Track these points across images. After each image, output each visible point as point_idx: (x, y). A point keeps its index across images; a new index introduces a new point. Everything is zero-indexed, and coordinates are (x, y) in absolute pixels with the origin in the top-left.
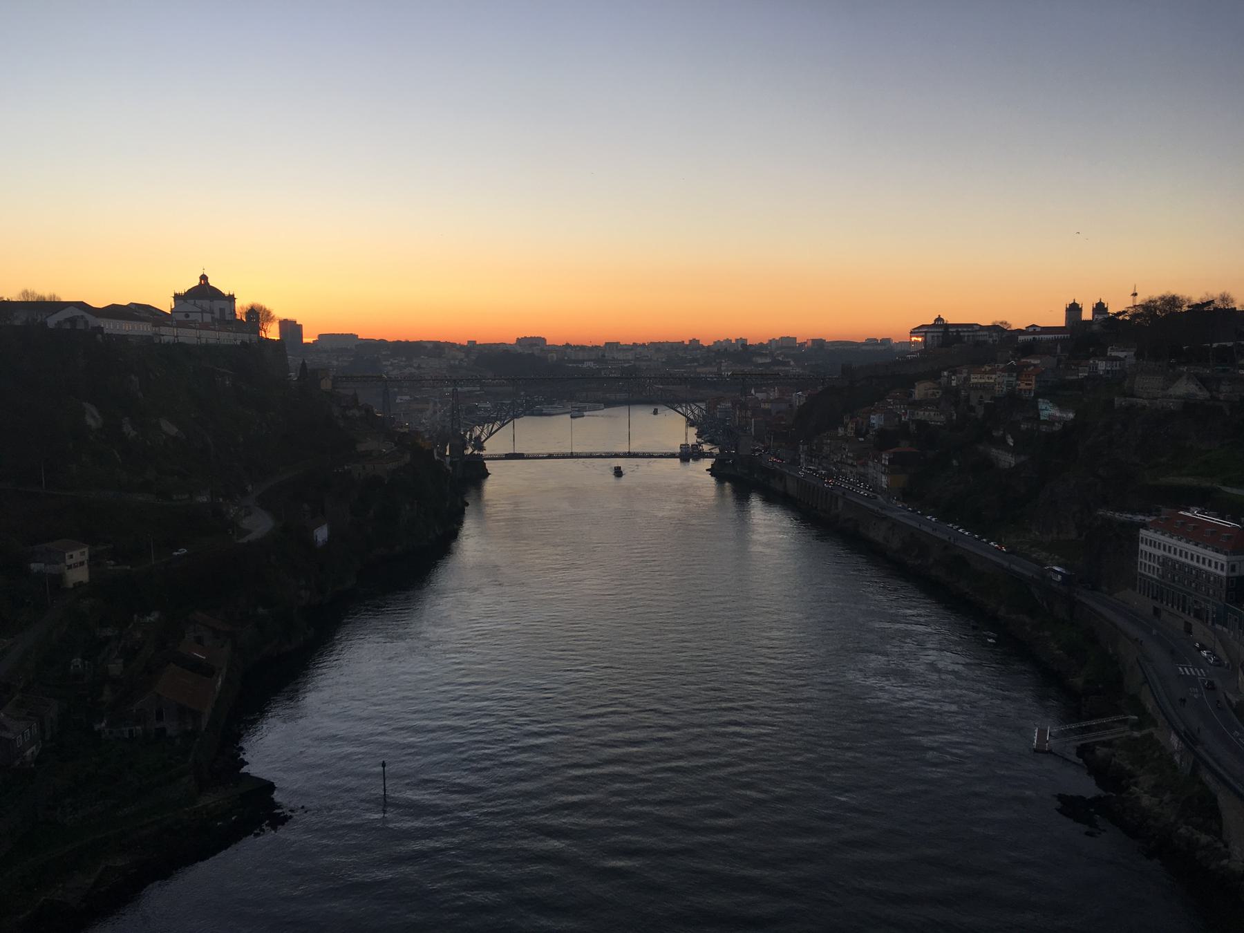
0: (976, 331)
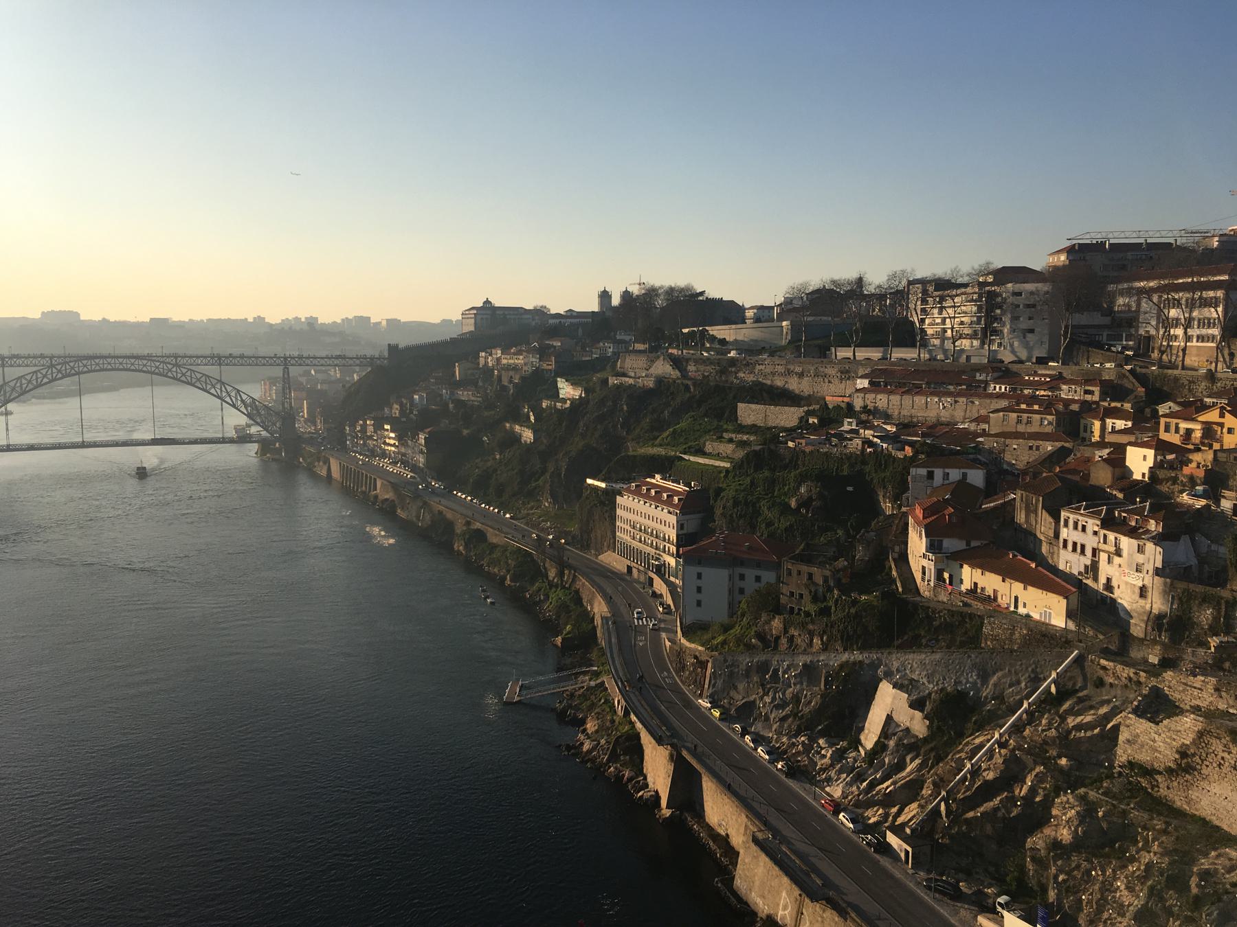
0: (522, 314)
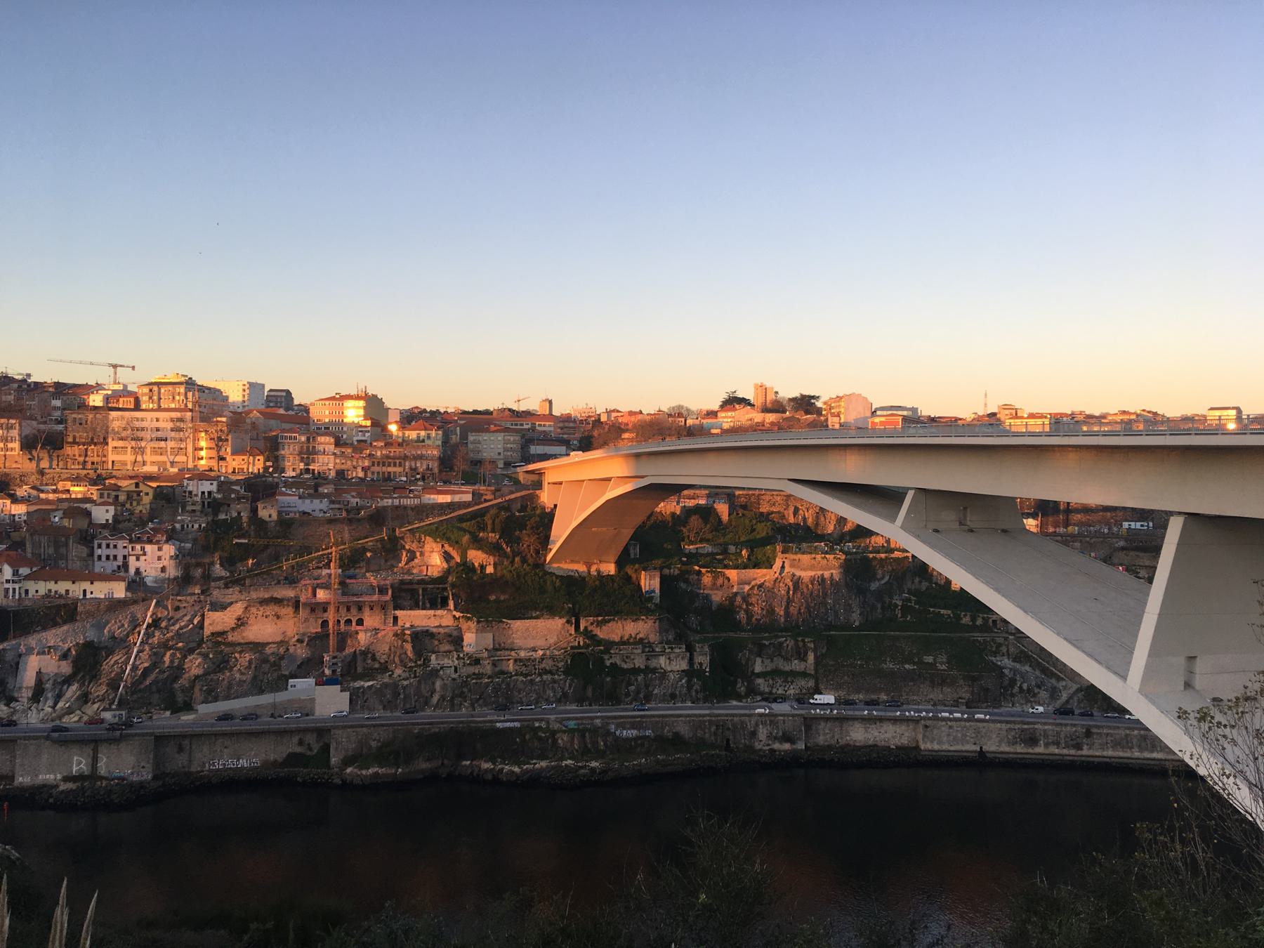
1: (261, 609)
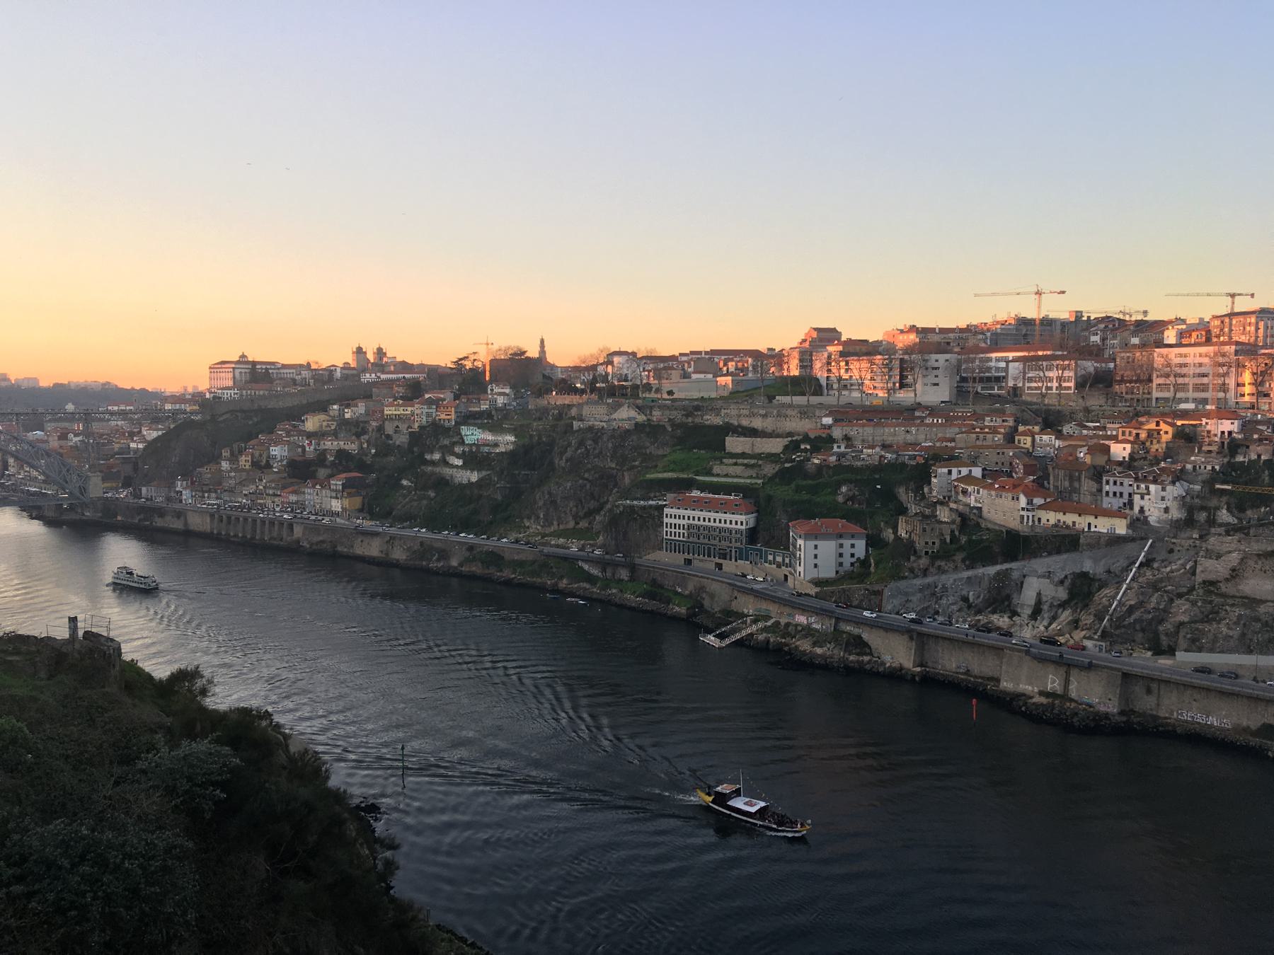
0: (278, 369)
1: (1260, 563)
